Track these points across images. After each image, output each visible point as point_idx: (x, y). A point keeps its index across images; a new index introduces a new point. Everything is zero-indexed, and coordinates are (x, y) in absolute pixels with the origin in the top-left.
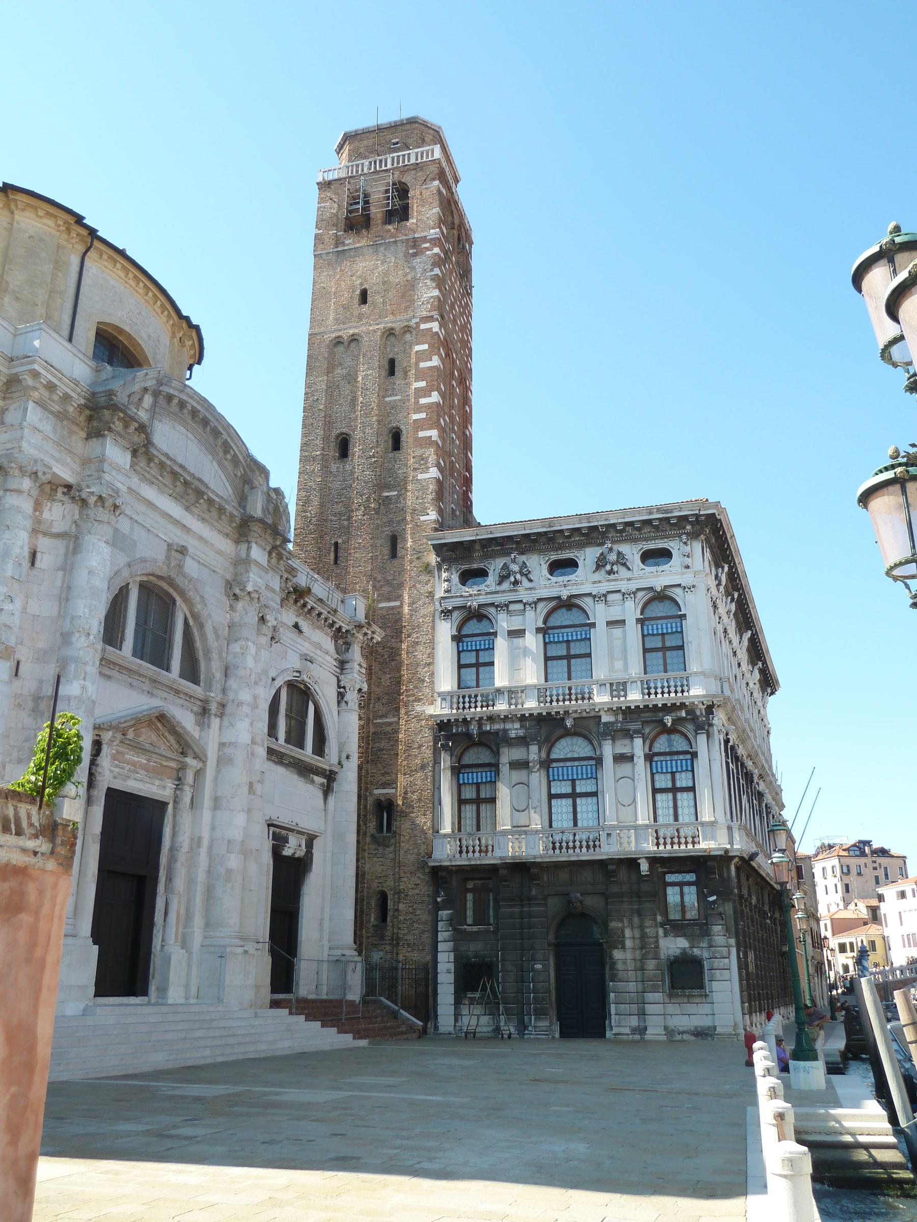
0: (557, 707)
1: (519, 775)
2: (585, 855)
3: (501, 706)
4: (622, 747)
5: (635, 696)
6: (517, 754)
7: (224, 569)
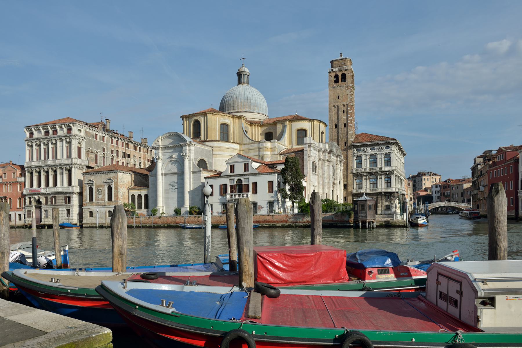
0: (371, 171)
1: (365, 181)
2: (375, 192)
3: (363, 170)
4: (381, 177)
5: (383, 169)
6: (365, 177)
7: (335, 161)
